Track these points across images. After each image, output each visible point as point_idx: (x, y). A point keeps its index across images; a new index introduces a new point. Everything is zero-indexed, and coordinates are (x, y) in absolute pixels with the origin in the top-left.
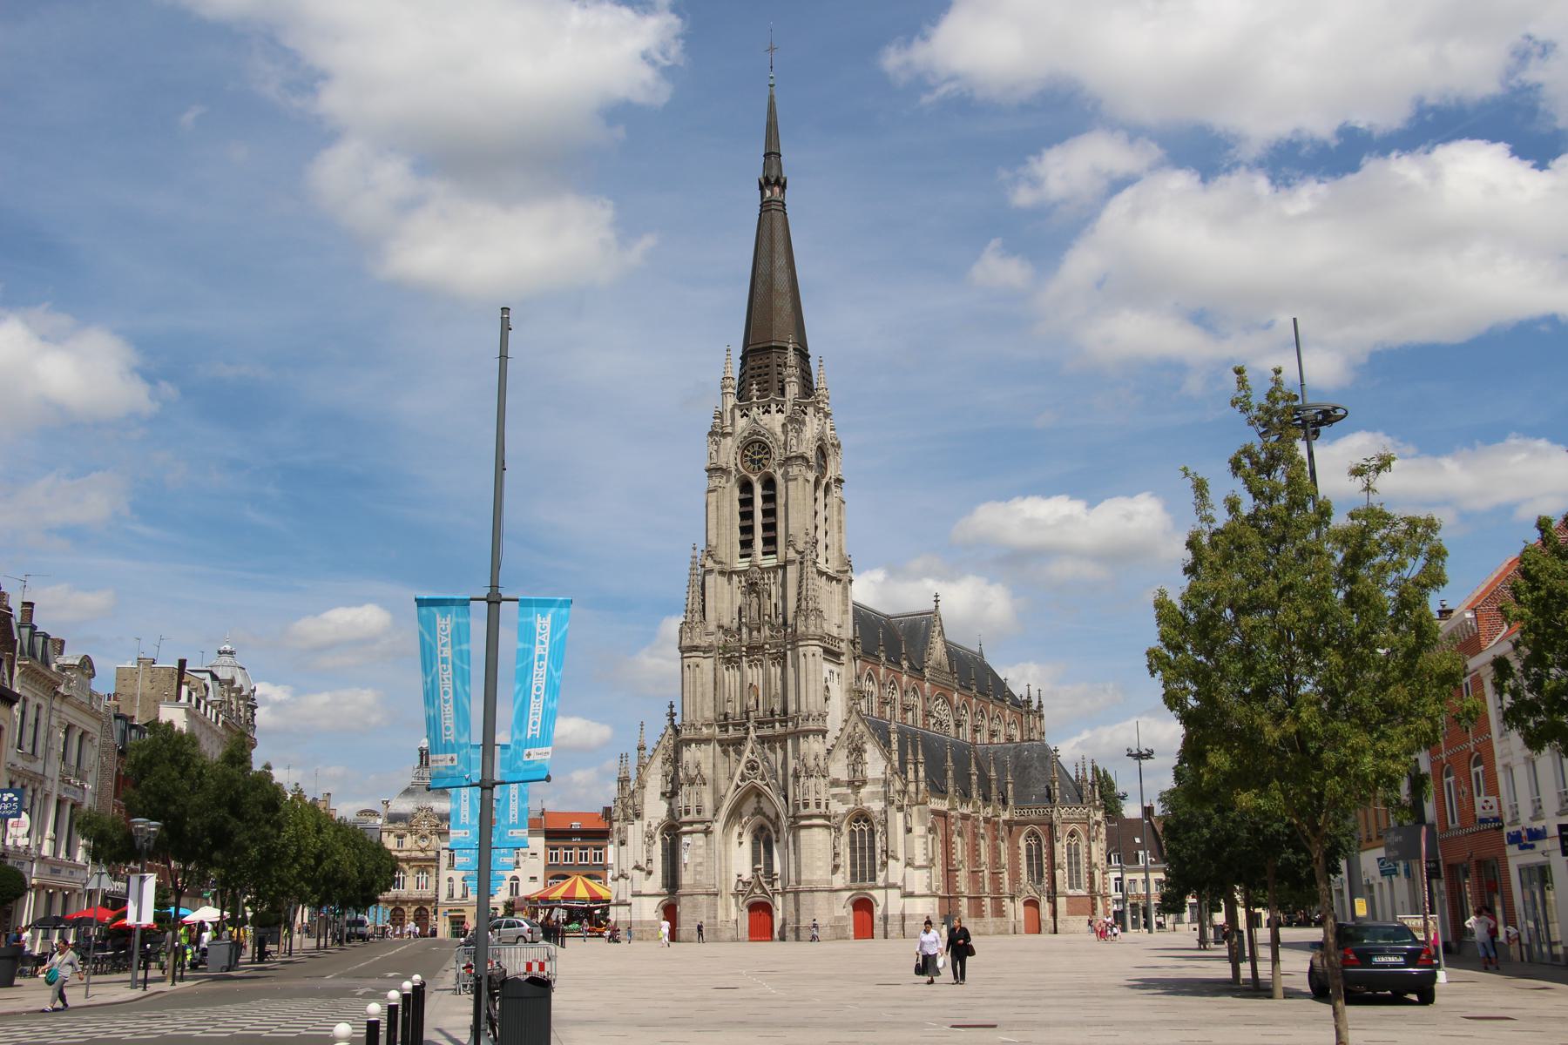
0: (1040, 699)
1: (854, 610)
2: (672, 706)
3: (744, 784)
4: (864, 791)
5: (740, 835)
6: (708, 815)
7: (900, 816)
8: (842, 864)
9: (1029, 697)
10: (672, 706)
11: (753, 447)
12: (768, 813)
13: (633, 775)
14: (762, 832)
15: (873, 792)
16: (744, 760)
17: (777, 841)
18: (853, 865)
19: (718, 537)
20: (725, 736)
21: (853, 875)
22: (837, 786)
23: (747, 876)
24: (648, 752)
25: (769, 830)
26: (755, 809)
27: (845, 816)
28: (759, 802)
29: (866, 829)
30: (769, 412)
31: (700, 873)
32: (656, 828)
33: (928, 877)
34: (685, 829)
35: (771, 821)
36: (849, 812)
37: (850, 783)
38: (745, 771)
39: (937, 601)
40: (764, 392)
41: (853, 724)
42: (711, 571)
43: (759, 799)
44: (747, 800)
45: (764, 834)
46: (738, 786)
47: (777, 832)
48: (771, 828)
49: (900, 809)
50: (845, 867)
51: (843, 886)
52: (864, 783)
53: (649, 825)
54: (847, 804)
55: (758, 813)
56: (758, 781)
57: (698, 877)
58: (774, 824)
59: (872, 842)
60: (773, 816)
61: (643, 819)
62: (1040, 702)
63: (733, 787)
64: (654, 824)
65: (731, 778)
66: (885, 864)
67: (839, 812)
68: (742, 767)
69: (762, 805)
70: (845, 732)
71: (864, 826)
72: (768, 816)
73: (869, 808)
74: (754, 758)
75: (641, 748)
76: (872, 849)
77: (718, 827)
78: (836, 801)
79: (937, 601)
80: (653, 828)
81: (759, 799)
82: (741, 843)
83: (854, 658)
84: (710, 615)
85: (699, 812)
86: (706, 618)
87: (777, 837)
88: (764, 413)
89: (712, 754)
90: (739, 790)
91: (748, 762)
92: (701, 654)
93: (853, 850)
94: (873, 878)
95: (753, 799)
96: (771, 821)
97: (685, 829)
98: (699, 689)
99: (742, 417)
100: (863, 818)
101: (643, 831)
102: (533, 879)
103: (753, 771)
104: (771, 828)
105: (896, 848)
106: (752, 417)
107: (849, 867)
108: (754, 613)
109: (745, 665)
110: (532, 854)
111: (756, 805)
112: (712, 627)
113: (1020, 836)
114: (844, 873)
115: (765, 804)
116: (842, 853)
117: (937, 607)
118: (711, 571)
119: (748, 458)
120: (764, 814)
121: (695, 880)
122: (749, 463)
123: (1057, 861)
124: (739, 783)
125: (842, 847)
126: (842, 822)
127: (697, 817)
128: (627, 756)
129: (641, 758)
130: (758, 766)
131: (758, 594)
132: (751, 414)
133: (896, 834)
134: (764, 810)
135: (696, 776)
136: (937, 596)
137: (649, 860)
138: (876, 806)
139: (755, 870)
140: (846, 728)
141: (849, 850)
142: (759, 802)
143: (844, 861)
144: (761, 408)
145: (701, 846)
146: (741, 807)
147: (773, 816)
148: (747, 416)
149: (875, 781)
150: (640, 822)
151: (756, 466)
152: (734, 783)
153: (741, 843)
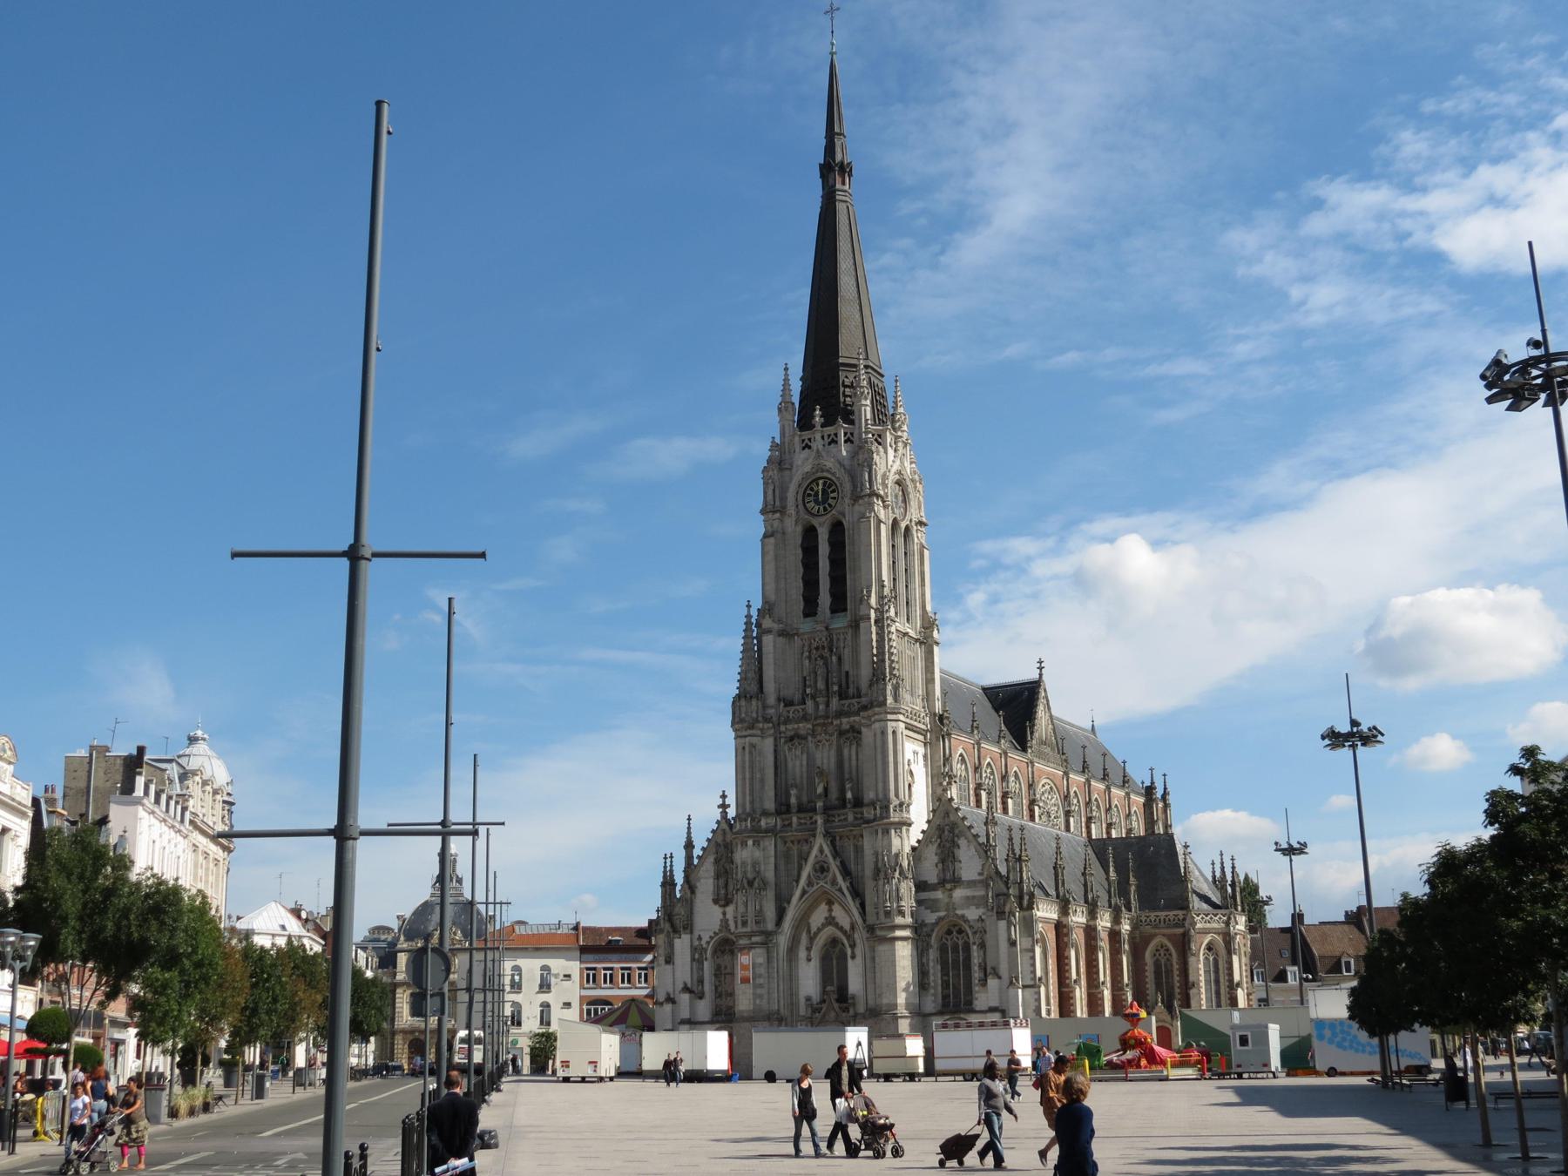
0: (1165, 785)
1: (942, 679)
2: (724, 796)
4: (959, 893)
5: (809, 949)
6: (770, 926)
7: (1002, 924)
8: (932, 984)
9: (1152, 783)
10: (724, 796)
11: (818, 485)
13: (679, 878)
14: (834, 947)
15: (968, 898)
17: (853, 957)
18: (945, 985)
21: (945, 997)
22: (924, 890)
23: (816, 997)
24: (697, 852)
25: (843, 944)
27: (937, 923)
28: (830, 910)
29: (960, 942)
30: (836, 442)
31: (761, 996)
32: (708, 943)
33: (1036, 1000)
34: (743, 942)
35: (845, 932)
36: (940, 919)
37: (942, 883)
39: (1041, 668)
40: (829, 421)
41: (942, 815)
42: (769, 631)
43: (830, 906)
44: (816, 907)
45: (837, 950)
46: (804, 892)
47: (853, 946)
48: (845, 942)
49: (1001, 914)
50: (935, 988)
51: (934, 1011)
52: (957, 881)
53: (700, 938)
54: (936, 912)
55: (830, 924)
56: (828, 886)
57: (758, 1002)
58: (848, 937)
59: (968, 959)
60: (847, 927)
61: (691, 933)
62: (1165, 789)
63: (798, 893)
64: (706, 938)
65: (797, 881)
66: (984, 982)
67: (927, 922)
68: (807, 870)
69: (833, 914)
71: (957, 938)
72: (842, 927)
73: (963, 916)
75: (689, 846)
76: (968, 967)
77: (783, 940)
78: (923, 908)
79: (1041, 668)
80: (703, 942)
81: (830, 906)
82: (809, 960)
83: (943, 737)
84: (770, 687)
86: (764, 690)
87: (853, 953)
88: (830, 444)
89: (773, 853)
90: (806, 896)
93: (945, 972)
94: (969, 1003)
95: (823, 907)
96: (845, 932)
97: (743, 942)
99: (804, 449)
100: (957, 928)
101: (691, 946)
102: (567, 1005)
104: (845, 942)
105: (998, 963)
106: (815, 448)
107: (940, 988)
108: (821, 685)
109: (811, 745)
110: (565, 976)
111: (826, 915)
112: (771, 700)
113: (1146, 949)
114: (935, 995)
115: (838, 912)
116: (931, 971)
117: (1041, 675)
118: (769, 631)
119: (812, 498)
120: (836, 925)
121: (754, 1004)
122: (812, 504)
123: (1191, 978)
125: (931, 964)
126: (933, 930)
127: (755, 928)
128: (671, 857)
129: (689, 858)
130: (828, 868)
132: (814, 445)
133: (997, 946)
134: (838, 920)
135: (755, 879)
136: (1041, 662)
137: (701, 981)
138: (972, 914)
139: (824, 992)
141: (939, 967)
142: (830, 910)
143: (934, 981)
144: (826, 438)
146: (809, 917)
147: (847, 927)
148: (810, 447)
149: (971, 884)
150: (688, 936)
151: (821, 508)
152: (800, 887)
153: (809, 960)
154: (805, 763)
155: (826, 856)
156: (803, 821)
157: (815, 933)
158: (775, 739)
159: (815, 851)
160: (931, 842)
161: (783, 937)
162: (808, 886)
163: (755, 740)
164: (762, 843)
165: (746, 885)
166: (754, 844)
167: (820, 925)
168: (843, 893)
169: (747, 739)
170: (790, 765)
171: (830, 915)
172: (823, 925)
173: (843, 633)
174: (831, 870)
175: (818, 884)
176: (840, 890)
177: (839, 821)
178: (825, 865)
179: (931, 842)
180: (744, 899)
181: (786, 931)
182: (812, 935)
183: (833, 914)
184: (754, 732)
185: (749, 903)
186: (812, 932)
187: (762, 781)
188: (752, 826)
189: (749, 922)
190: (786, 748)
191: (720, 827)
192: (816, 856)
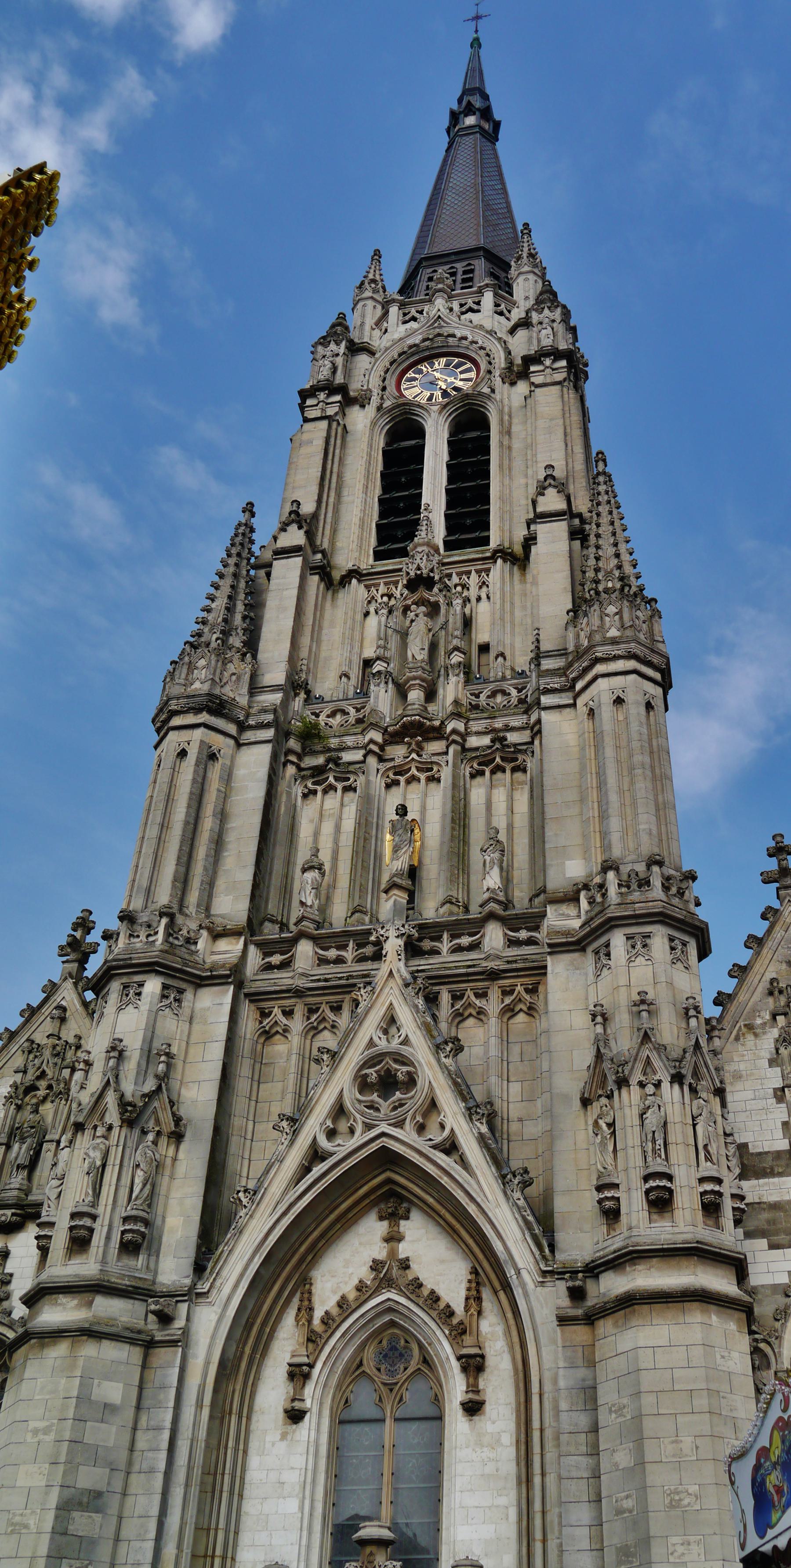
3: (344, 1145)
12: (430, 1283)
16: (353, 1057)
17: (473, 1408)
19: (319, 501)
20: (284, 979)
26: (376, 1266)
28: (394, 1238)
38: (351, 1097)
46: (316, 1155)
58: (459, 1332)
65: (295, 1121)
69: (404, 1250)
70: (753, 977)
72: (434, 1298)
74: (395, 1044)
82: (295, 1416)
85: (129, 1248)
87: (473, 1388)
90: (318, 1170)
91: (370, 1062)
92: (232, 729)
98: (208, 823)
103: (385, 1096)
111: (380, 1252)
124: (324, 1143)
130: (411, 1081)
131: (434, 610)
134: (418, 1270)
140: (758, 968)
145: (109, 1408)
153: (295, 1416)
154: (349, 825)
155: (406, 1042)
156: (332, 953)
157: (327, 1319)
158: (274, 757)
159: (370, 1028)
160: (750, 1027)
161: (216, 1310)
162: (331, 1134)
163: (218, 741)
164: (188, 995)
165: (113, 1116)
166: (164, 996)
167: (349, 1289)
168: (463, 1162)
169: (199, 733)
170: (305, 831)
171: (392, 1253)
172: (360, 1287)
173: (478, 572)
174: (421, 1083)
175: (368, 1127)
176: (450, 1147)
177: (459, 949)
178: (401, 1071)
179: (750, 1027)
180: (97, 1156)
181: (227, 1290)
182: (316, 1321)
183: (404, 1250)
184: (220, 723)
185: (110, 1176)
186: (318, 1314)
187: (218, 843)
188: (166, 940)
189: (98, 1240)
190: (298, 790)
191: (57, 999)
192: (371, 1043)
